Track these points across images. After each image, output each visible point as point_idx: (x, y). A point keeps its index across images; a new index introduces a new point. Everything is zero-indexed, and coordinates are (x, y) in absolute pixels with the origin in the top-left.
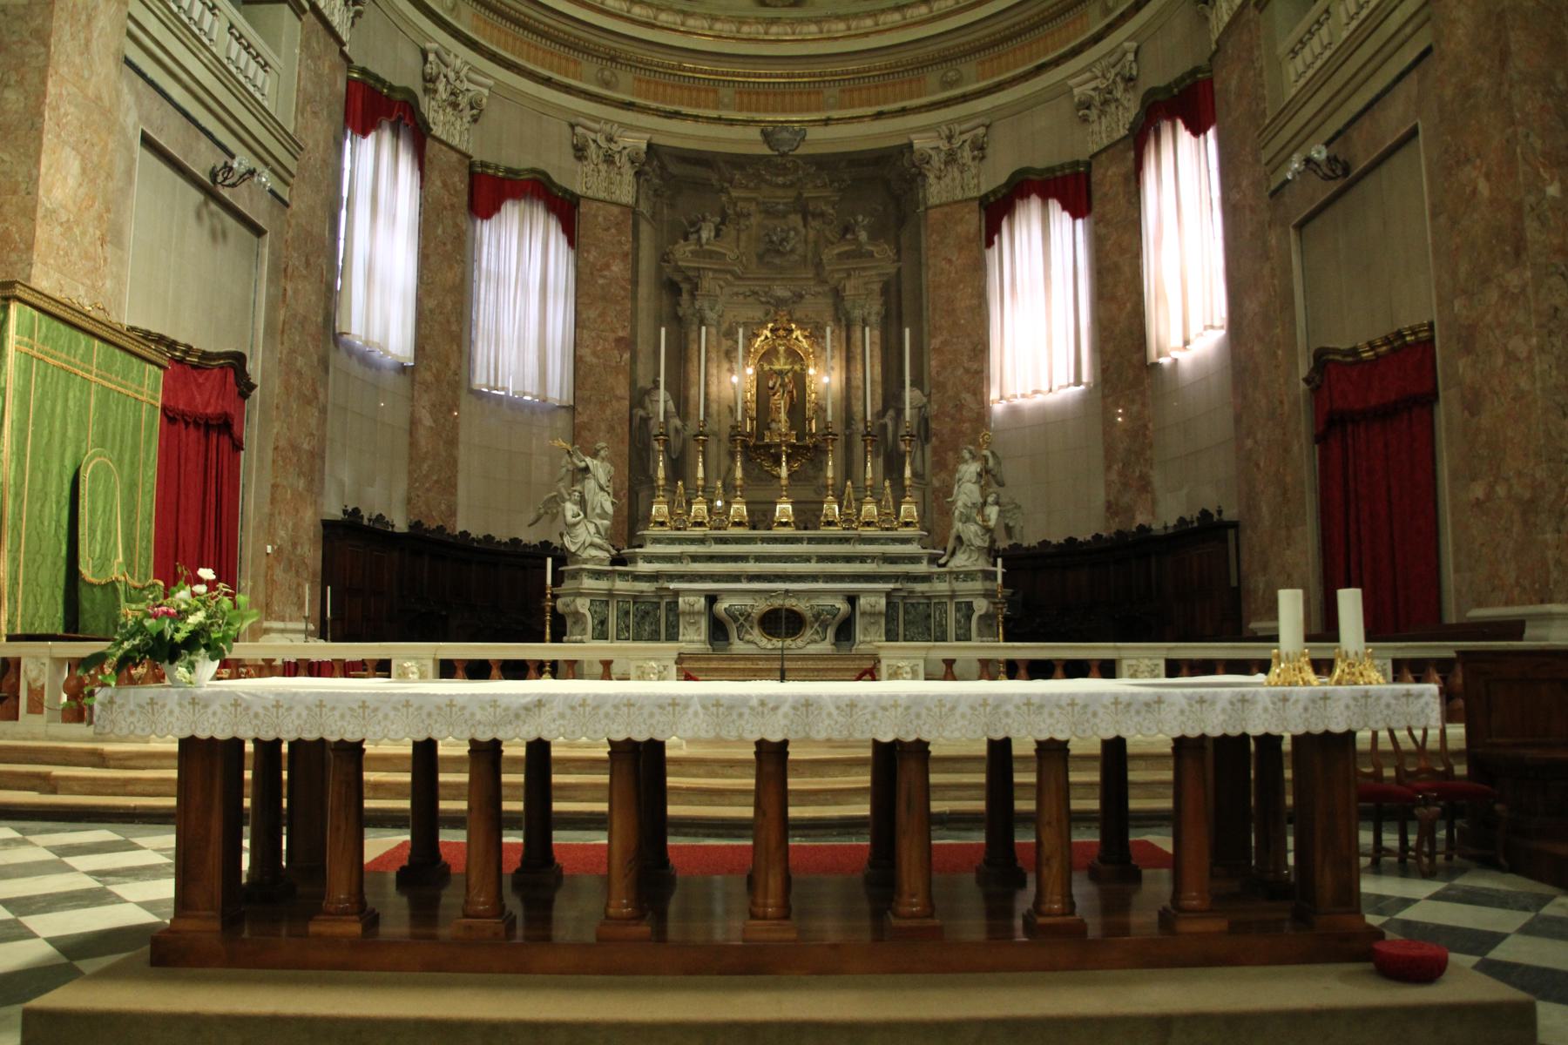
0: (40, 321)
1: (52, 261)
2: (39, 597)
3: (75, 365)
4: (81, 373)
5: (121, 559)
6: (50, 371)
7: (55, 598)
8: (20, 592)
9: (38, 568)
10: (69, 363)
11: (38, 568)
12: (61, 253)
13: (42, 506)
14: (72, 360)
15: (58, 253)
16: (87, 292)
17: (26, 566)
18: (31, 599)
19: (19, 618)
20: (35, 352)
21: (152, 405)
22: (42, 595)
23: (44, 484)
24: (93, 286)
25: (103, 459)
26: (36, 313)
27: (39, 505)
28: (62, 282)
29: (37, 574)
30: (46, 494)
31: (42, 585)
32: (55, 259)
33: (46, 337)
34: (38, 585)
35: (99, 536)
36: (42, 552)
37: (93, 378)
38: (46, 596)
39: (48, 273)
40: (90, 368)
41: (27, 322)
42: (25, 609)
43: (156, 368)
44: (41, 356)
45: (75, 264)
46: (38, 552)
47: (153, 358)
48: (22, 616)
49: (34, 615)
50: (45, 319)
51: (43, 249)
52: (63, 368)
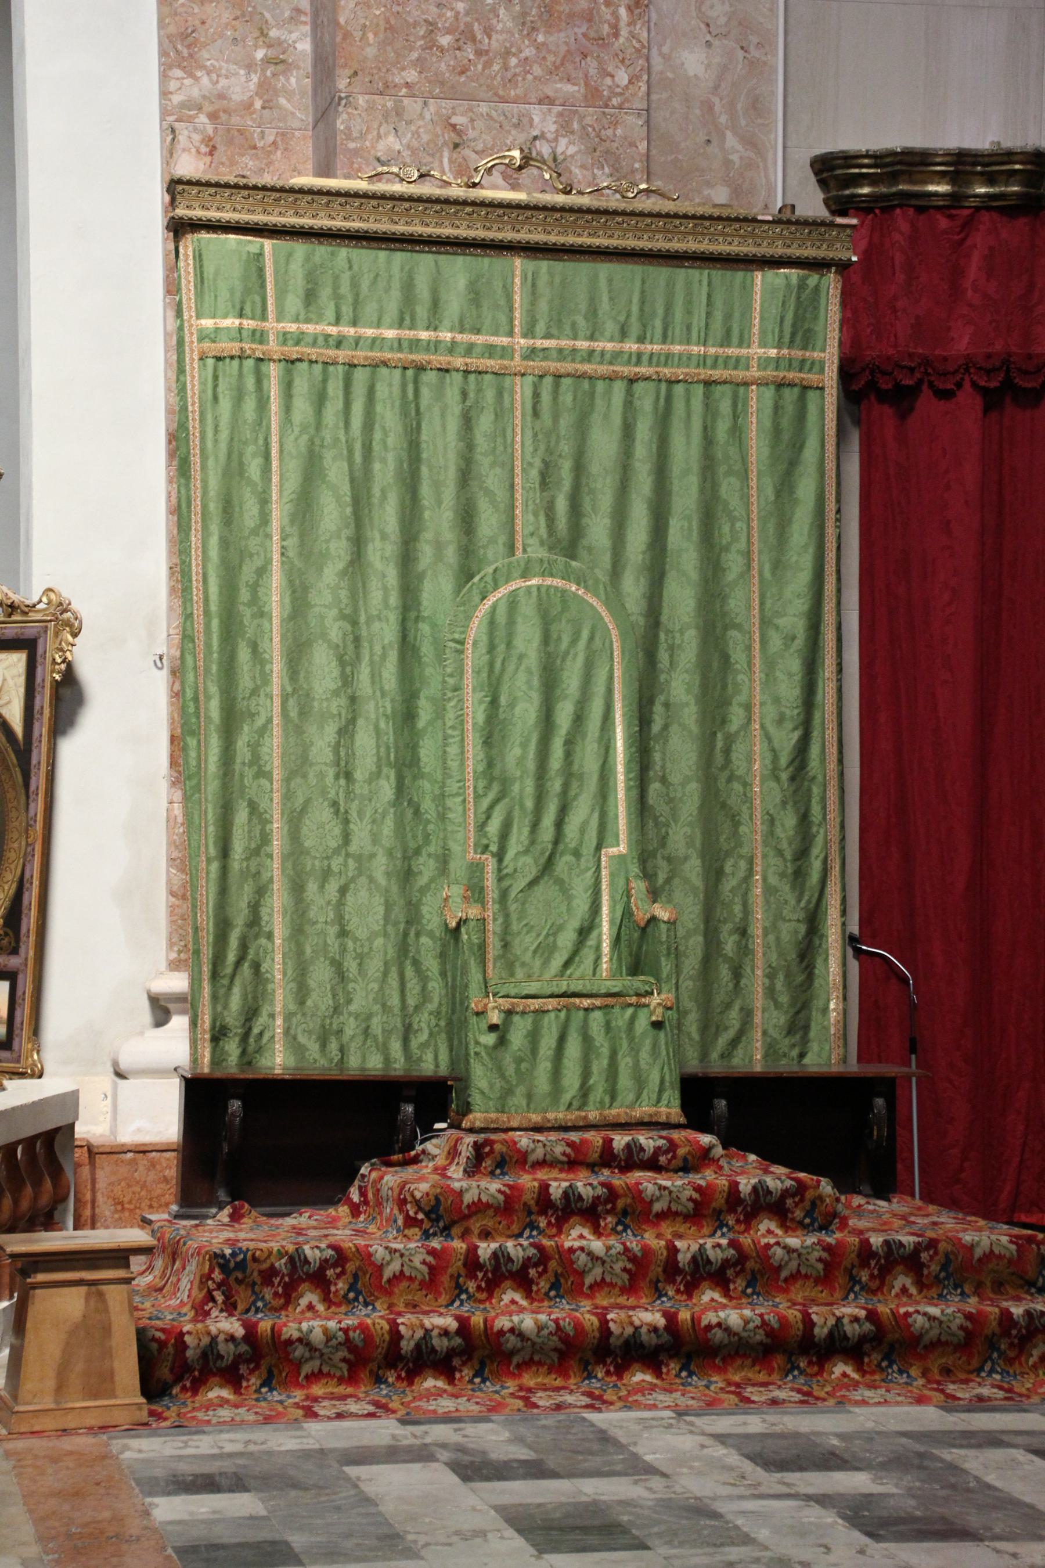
0: (283, 263)
1: (411, 75)
2: (351, 965)
3: (435, 346)
4: (459, 362)
5: (622, 848)
6: (335, 389)
7: (416, 963)
8: (278, 957)
9: (343, 891)
10: (415, 344)
11: (343, 891)
12: (445, 40)
13: (347, 731)
14: (424, 335)
15: (431, 44)
16: (565, 127)
17: (297, 888)
18: (321, 974)
19: (279, 1021)
20: (273, 346)
21: (780, 385)
22: (361, 958)
23: (347, 680)
24: (593, 95)
25: (557, 582)
26: (268, 245)
27: (331, 730)
28: (457, 120)
29: (340, 904)
30: (353, 699)
31: (362, 933)
32: (420, 64)
33: (310, 297)
34: (343, 933)
35: (525, 788)
36: (353, 848)
37: (517, 362)
38: (375, 966)
39: (399, 112)
40: (504, 340)
41: (234, 272)
42: (301, 993)
43: (794, 274)
44: (294, 352)
45: (508, 53)
46: (336, 851)
47: (779, 250)
48: (288, 1017)
49: (336, 1010)
50: (300, 248)
51: (370, 52)
52: (385, 363)
